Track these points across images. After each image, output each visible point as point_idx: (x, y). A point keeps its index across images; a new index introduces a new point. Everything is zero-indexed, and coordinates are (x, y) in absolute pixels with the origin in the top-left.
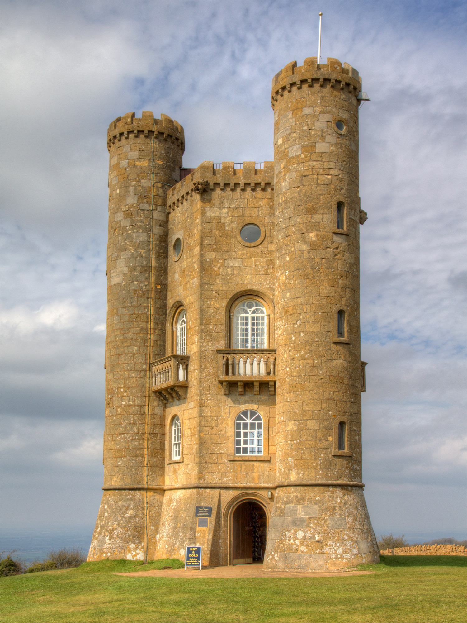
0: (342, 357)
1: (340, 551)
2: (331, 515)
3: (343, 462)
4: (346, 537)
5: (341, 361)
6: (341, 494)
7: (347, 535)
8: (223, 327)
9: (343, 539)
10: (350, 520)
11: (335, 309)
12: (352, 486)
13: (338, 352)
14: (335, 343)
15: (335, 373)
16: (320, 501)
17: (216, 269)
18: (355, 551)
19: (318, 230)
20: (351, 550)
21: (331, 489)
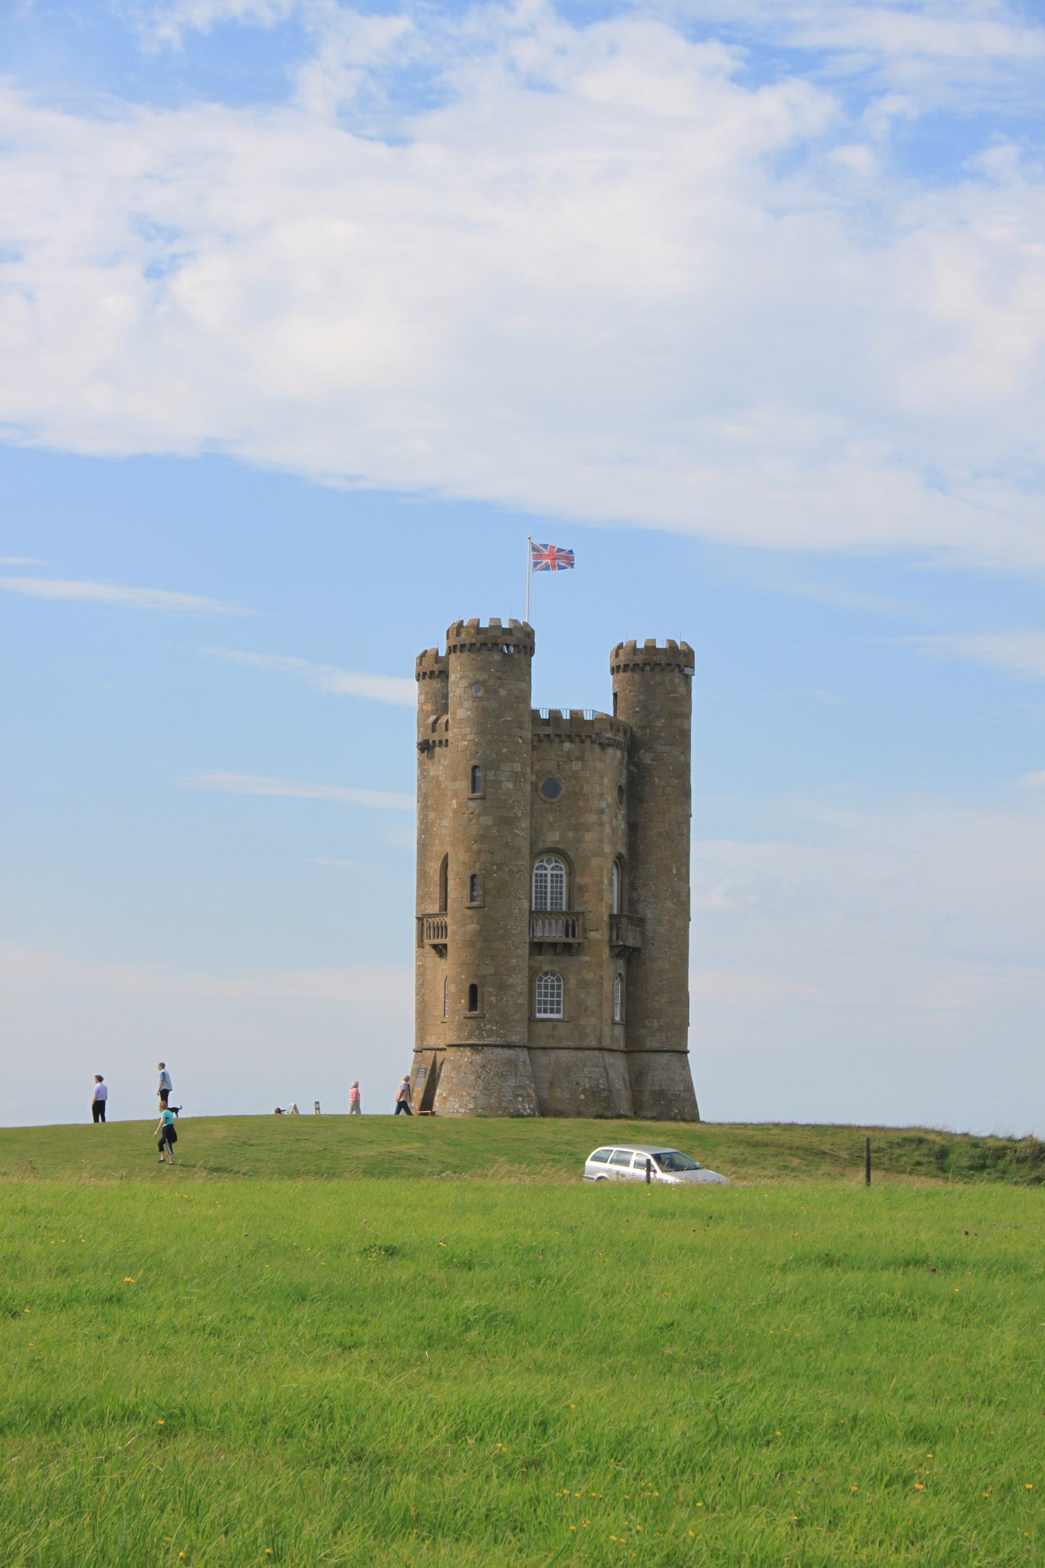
0: (475, 920)
1: (457, 1106)
2: (457, 1073)
3: (474, 1023)
4: (465, 1094)
5: (474, 925)
6: (469, 1054)
7: (467, 1092)
8: (437, 889)
9: (462, 1095)
10: (472, 1078)
11: (469, 873)
12: (483, 1046)
13: (471, 917)
14: (468, 908)
15: (467, 939)
16: (452, 1060)
17: (435, 829)
18: (471, 1106)
19: (457, 798)
20: (466, 1105)
21: (462, 1049)
